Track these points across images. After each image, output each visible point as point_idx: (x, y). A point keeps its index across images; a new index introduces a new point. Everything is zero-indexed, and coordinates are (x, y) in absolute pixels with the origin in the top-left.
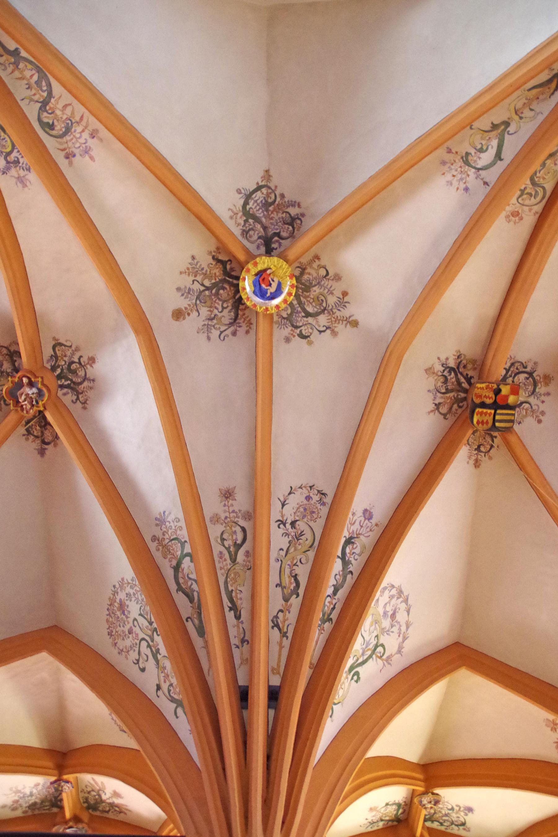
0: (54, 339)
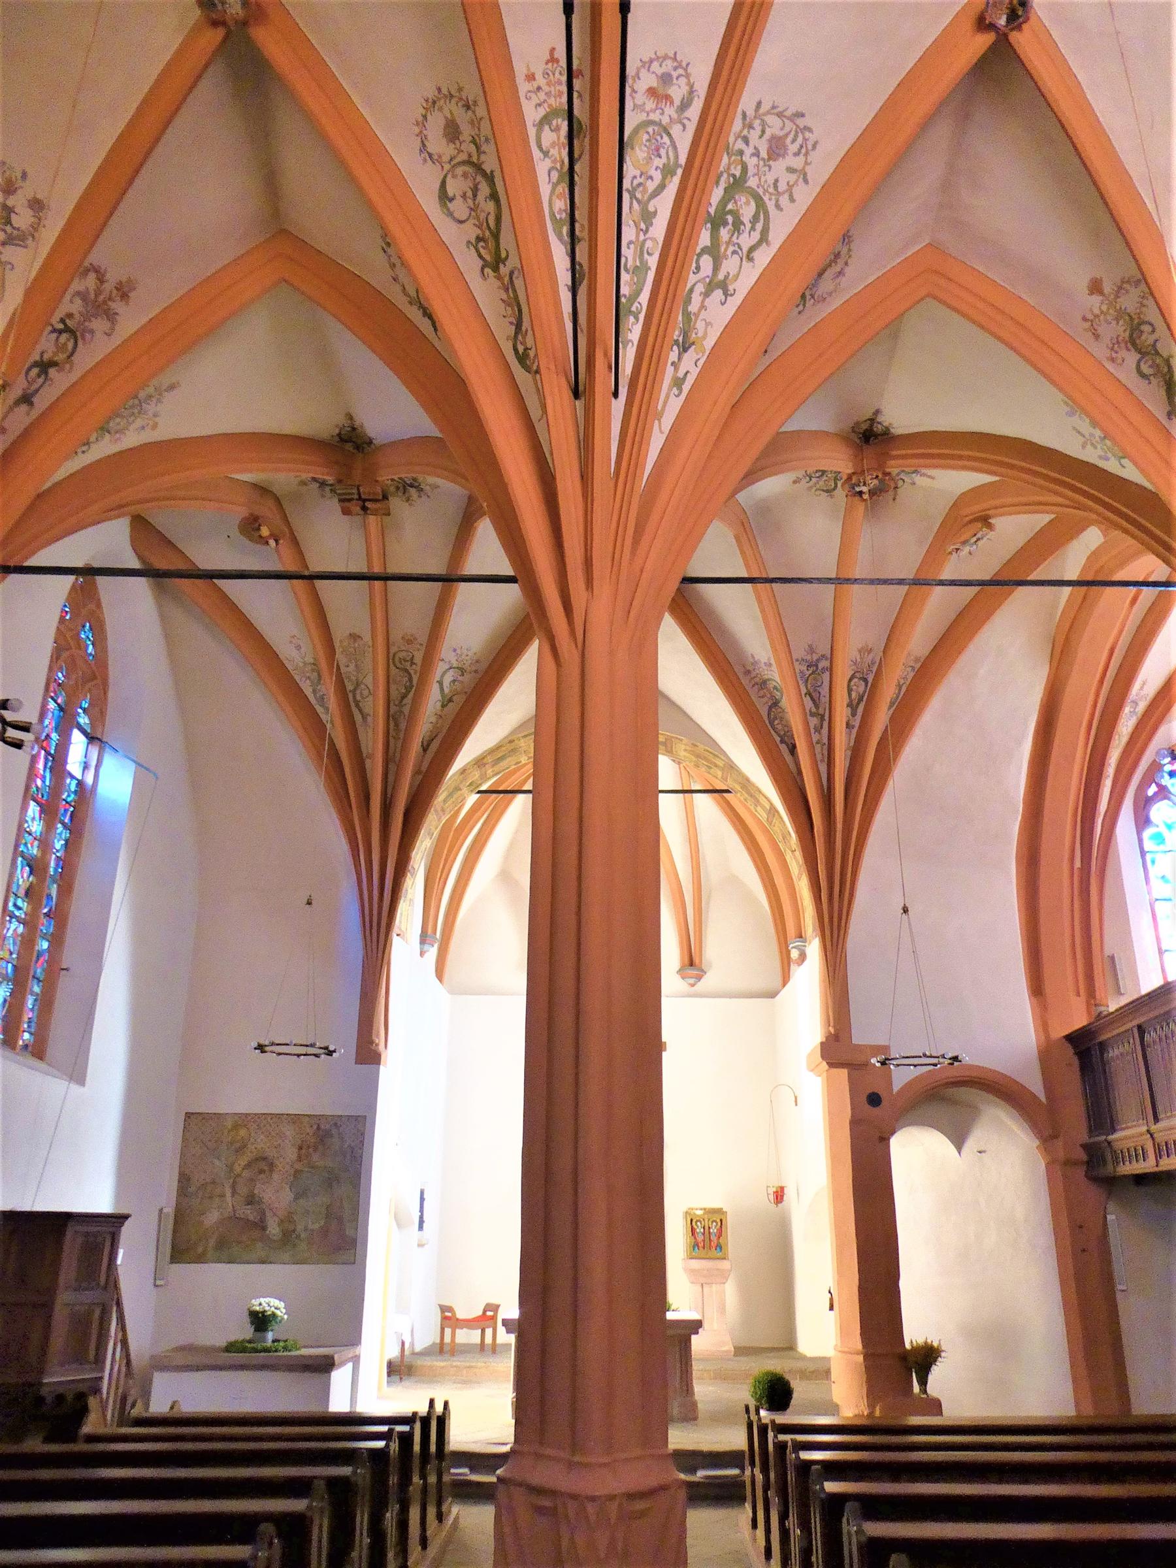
0: (832, 497)
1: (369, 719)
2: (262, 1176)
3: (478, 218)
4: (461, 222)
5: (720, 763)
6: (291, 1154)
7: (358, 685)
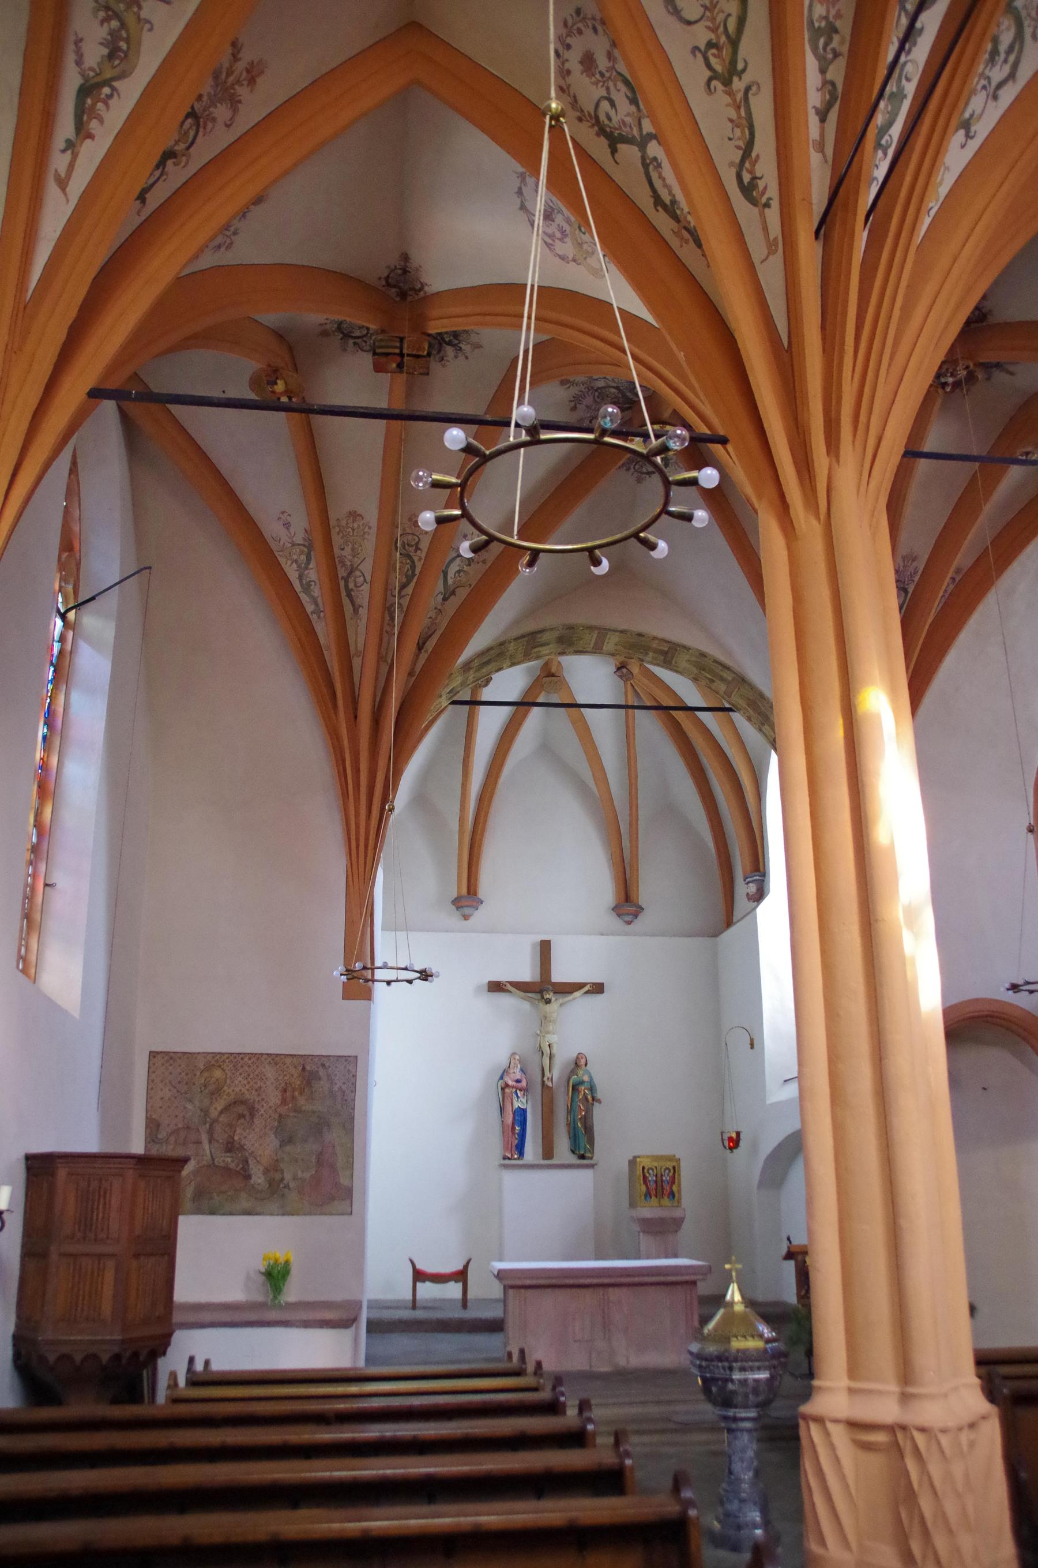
1: (363, 612)
2: (242, 1120)
3: (713, 19)
4: (689, 23)
5: (728, 676)
6: (274, 1097)
7: (350, 574)
